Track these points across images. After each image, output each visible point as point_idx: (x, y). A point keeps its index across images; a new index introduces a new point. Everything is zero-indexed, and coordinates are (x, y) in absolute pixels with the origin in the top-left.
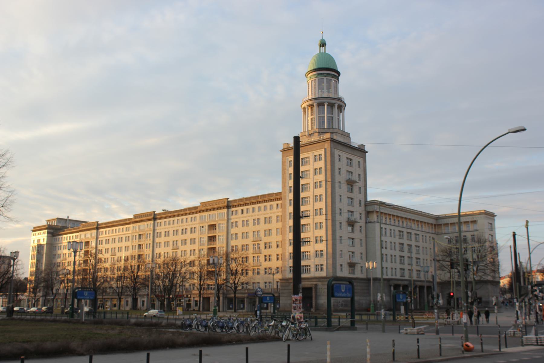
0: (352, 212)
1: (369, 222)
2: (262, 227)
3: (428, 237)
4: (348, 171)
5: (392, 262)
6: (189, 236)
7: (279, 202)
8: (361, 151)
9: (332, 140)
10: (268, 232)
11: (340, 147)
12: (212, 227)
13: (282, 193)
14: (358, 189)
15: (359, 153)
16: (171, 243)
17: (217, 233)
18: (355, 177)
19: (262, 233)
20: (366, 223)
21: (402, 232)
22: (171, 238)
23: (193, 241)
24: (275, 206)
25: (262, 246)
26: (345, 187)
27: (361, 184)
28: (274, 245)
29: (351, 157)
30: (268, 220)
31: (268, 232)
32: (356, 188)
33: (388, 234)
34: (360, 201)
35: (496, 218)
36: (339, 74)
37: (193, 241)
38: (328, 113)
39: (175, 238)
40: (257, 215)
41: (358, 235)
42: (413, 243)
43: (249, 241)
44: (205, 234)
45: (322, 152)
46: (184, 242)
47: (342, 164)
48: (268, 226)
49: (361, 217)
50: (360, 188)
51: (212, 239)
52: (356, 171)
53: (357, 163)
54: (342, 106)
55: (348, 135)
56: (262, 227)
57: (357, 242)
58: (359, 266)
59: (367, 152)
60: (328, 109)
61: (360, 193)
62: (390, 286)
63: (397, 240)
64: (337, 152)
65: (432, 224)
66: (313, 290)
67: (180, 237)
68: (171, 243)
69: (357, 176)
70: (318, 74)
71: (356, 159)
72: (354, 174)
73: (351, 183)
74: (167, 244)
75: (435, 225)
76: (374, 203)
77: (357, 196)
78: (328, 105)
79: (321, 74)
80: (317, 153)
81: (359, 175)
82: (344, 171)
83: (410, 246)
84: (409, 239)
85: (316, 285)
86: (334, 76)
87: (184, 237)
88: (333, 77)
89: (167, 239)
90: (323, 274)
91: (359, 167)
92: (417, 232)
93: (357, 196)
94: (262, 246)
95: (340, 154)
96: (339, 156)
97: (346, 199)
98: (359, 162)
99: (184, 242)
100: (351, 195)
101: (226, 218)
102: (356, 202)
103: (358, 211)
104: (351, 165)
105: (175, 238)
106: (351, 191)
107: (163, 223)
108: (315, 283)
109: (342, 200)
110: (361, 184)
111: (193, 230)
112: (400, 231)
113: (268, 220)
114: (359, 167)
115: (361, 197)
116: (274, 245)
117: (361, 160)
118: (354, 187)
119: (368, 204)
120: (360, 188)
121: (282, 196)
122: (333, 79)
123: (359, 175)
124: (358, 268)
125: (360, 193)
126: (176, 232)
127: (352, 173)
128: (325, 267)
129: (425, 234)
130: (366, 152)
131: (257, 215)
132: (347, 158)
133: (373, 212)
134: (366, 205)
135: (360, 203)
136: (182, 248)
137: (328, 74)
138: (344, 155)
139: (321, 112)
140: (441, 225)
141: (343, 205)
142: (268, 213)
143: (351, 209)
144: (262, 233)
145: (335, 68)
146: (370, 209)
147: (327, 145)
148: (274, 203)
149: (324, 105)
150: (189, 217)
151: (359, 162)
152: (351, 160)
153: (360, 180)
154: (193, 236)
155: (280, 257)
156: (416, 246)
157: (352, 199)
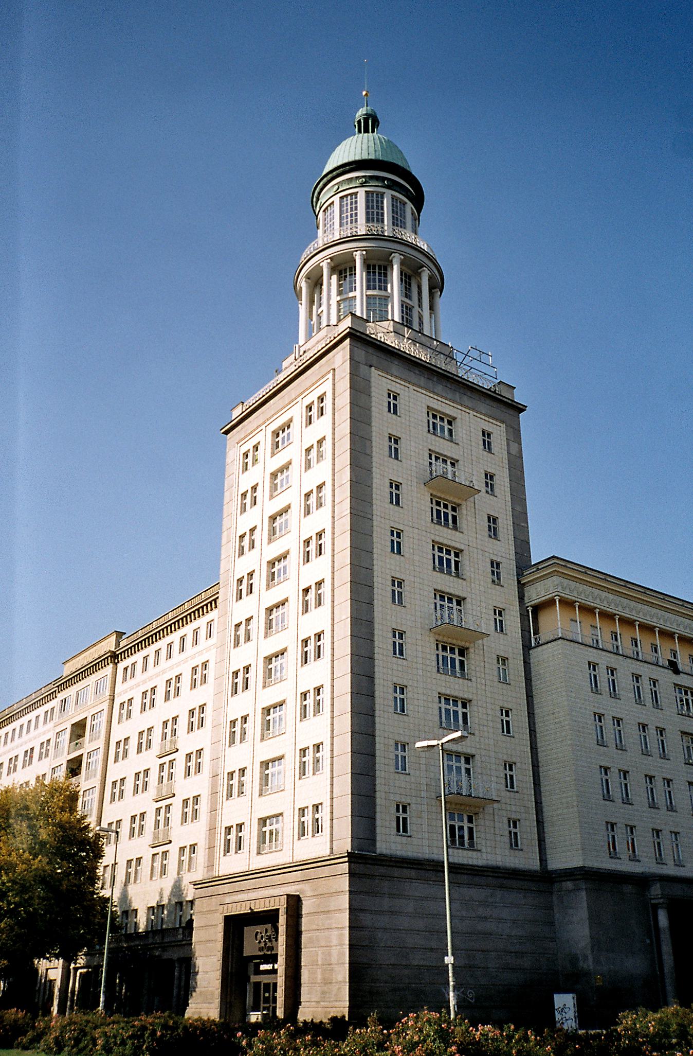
1: (538, 645)
5: (653, 806)
11: (395, 367)
20: (527, 648)
40: (181, 664)
59: (520, 409)
62: (655, 908)
64: (381, 383)
71: (470, 422)
85: (295, 903)
86: (393, 185)
88: (388, 187)
90: (316, 847)
93: (470, 536)
95: (396, 388)
98: (486, 434)
102: (476, 567)
108: (292, 890)
115: (505, 550)
122: (389, 193)
123: (489, 477)
128: (324, 815)
130: (520, 409)
133: (550, 603)
138: (417, 400)
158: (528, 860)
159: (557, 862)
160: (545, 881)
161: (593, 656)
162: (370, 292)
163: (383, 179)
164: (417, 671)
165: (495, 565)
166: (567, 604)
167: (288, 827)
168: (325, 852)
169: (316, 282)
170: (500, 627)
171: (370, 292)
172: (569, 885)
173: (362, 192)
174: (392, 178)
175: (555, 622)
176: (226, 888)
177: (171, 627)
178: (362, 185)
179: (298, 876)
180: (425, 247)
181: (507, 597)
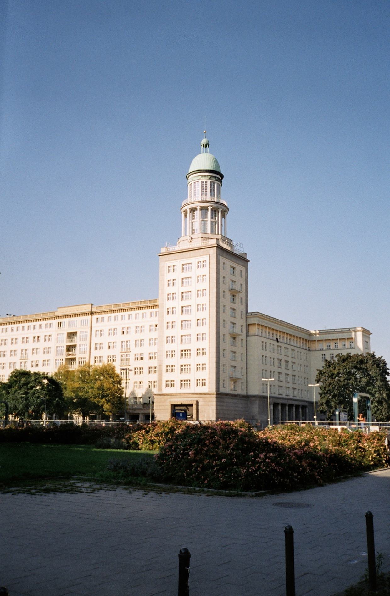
0: (234, 324)
2: (132, 337)
3: (302, 353)
4: (232, 281)
6: (42, 344)
7: (154, 310)
8: (242, 259)
9: (219, 247)
10: (139, 343)
12: (72, 335)
14: (240, 300)
15: (242, 262)
16: (19, 352)
17: (77, 341)
18: (237, 287)
19: (132, 344)
20: (247, 336)
22: (19, 347)
23: (47, 350)
24: (148, 314)
25: (132, 358)
27: (243, 295)
28: (146, 357)
29: (234, 266)
30: (140, 329)
31: (139, 343)
32: (238, 300)
33: (268, 349)
34: (242, 312)
35: (371, 336)
36: (222, 176)
37: (47, 350)
38: (212, 218)
39: (25, 346)
40: (126, 323)
41: (240, 349)
43: (116, 352)
44: (63, 341)
45: (206, 258)
46: (34, 351)
47: (226, 272)
48: (139, 336)
50: (242, 298)
51: (70, 348)
52: (240, 281)
53: (240, 272)
54: (225, 211)
55: (230, 243)
56: (132, 337)
57: (238, 355)
58: (241, 381)
59: (248, 261)
60: (212, 213)
61: (242, 304)
63: (276, 356)
64: (222, 260)
65: (306, 340)
66: (194, 406)
67: (31, 345)
68: (19, 352)
69: (240, 286)
70: (202, 176)
71: (239, 268)
72: (236, 283)
73: (234, 294)
74: (13, 353)
75: (308, 341)
76: (257, 315)
77: (240, 308)
78: (212, 210)
79: (205, 176)
80: (201, 259)
81: (241, 285)
82: (227, 280)
83: (287, 362)
85: (197, 402)
87: (36, 345)
89: (14, 347)
90: (205, 389)
91: (241, 277)
92: (294, 348)
94: (132, 358)
97: (229, 310)
98: (241, 271)
99: (34, 351)
100: (234, 306)
101: (89, 326)
103: (240, 322)
104: (233, 274)
105: (25, 346)
106: (233, 301)
107: (10, 330)
109: (225, 311)
110: (243, 295)
111: (48, 338)
113: (140, 329)
114: (241, 277)
115: (244, 307)
116: (146, 357)
117: (243, 269)
118: (237, 297)
119: (248, 315)
120: (242, 298)
121: (159, 303)
123: (241, 285)
124: (239, 385)
125: (242, 304)
126: (26, 340)
127: (234, 282)
130: (248, 261)
131: (126, 323)
132: (231, 267)
135: (242, 315)
136: (32, 358)
139: (204, 216)
141: (226, 316)
142: (140, 322)
143: (233, 320)
144: (132, 344)
145: (218, 171)
146: (251, 321)
147: (213, 251)
148: (148, 311)
149: (207, 209)
150: (43, 323)
151: (241, 271)
152: (234, 268)
154: (47, 344)
155: (153, 370)
157: (234, 310)
158: (244, 393)
159: (250, 393)
160: (248, 398)
161: (263, 339)
162: (212, 220)
163: (216, 177)
164: (227, 345)
167: (193, 383)
168: (207, 391)
169: (193, 210)
171: (212, 220)
172: (254, 399)
173: (209, 181)
174: (216, 175)
175: (254, 330)
176: (168, 397)
177: (124, 310)
178: (209, 179)
179: (198, 396)
180: (226, 204)
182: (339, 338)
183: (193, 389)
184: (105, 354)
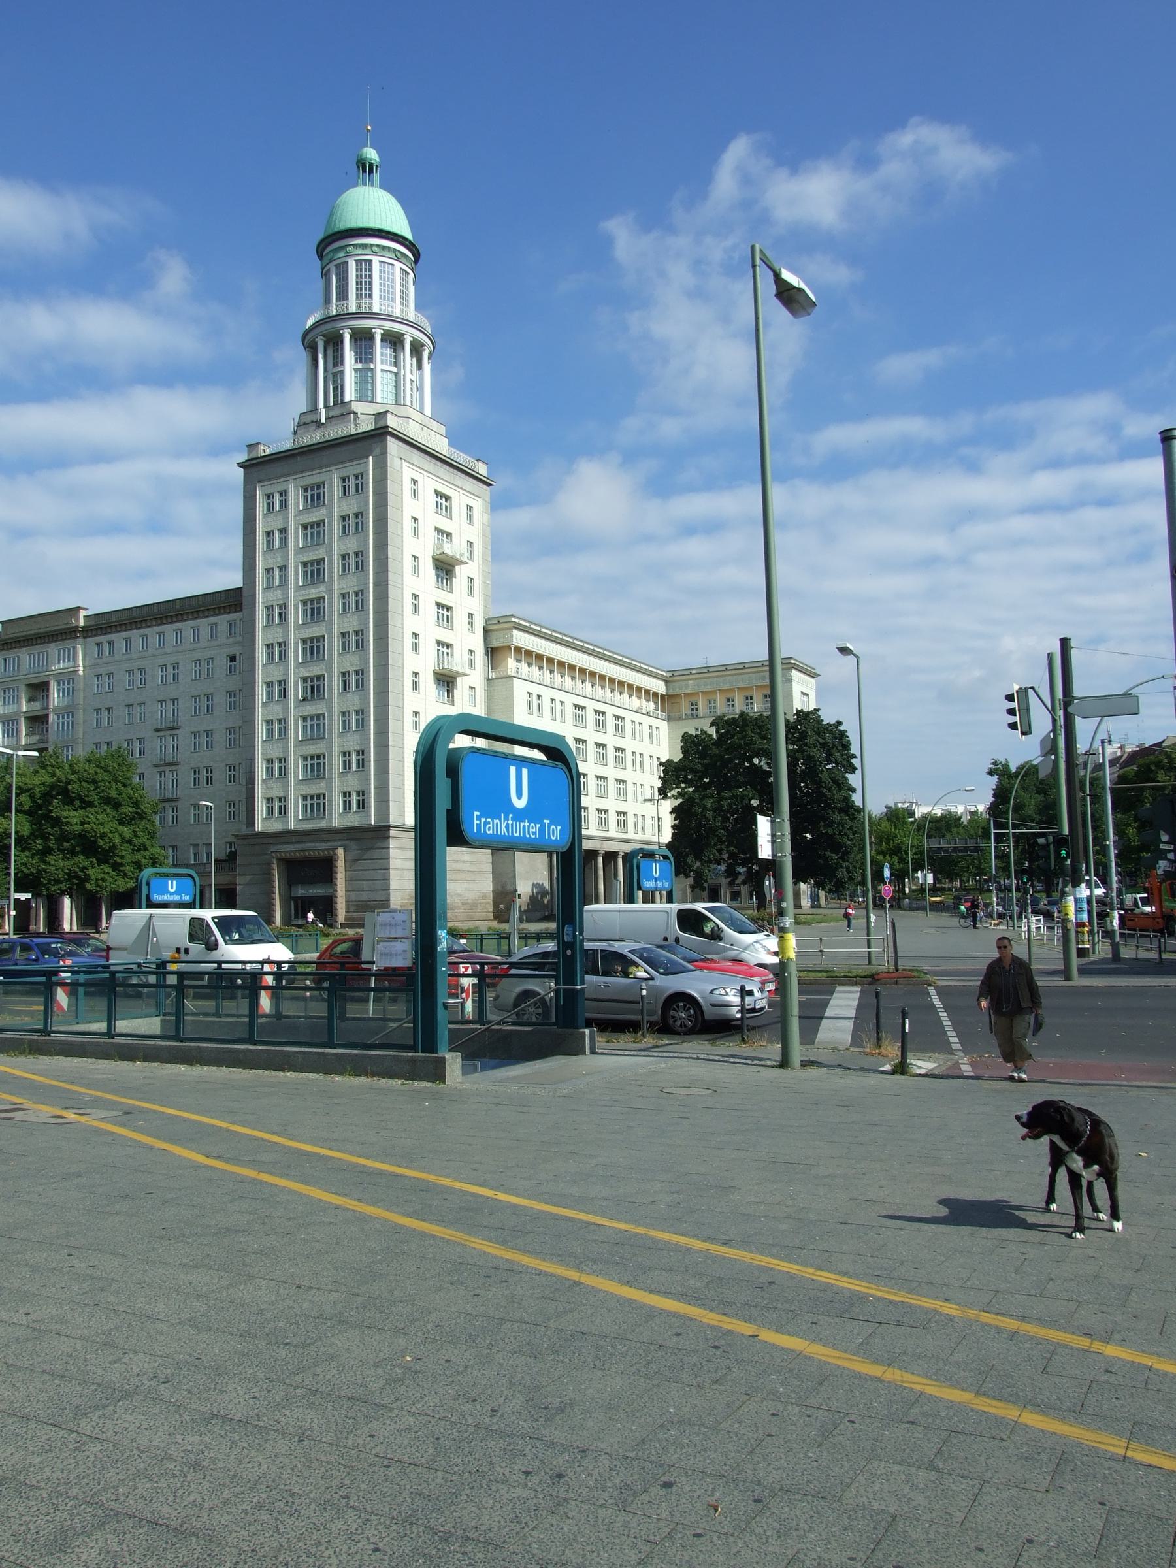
11: (416, 456)
13: (245, 594)
21: (583, 708)
26: (428, 570)
34: (471, 616)
42: (610, 740)
49: (472, 664)
65: (655, 694)
79: (365, 246)
84: (600, 725)
86: (400, 257)
96: (415, 482)
98: (470, 508)
104: (448, 513)
112: (577, 706)
122: (398, 265)
123: (470, 544)
127: (449, 535)
129: (638, 718)
134: (486, 631)
137: (384, 247)
138: (429, 485)
140: (680, 695)
151: (470, 508)
152: (448, 498)
153: (471, 558)
156: (617, 749)
163: (395, 250)
165: (471, 616)
166: (518, 650)
170: (472, 664)
176: (271, 841)
178: (376, 254)
181: (476, 641)
182: (735, 685)
183: (337, 818)
184: (118, 738)
